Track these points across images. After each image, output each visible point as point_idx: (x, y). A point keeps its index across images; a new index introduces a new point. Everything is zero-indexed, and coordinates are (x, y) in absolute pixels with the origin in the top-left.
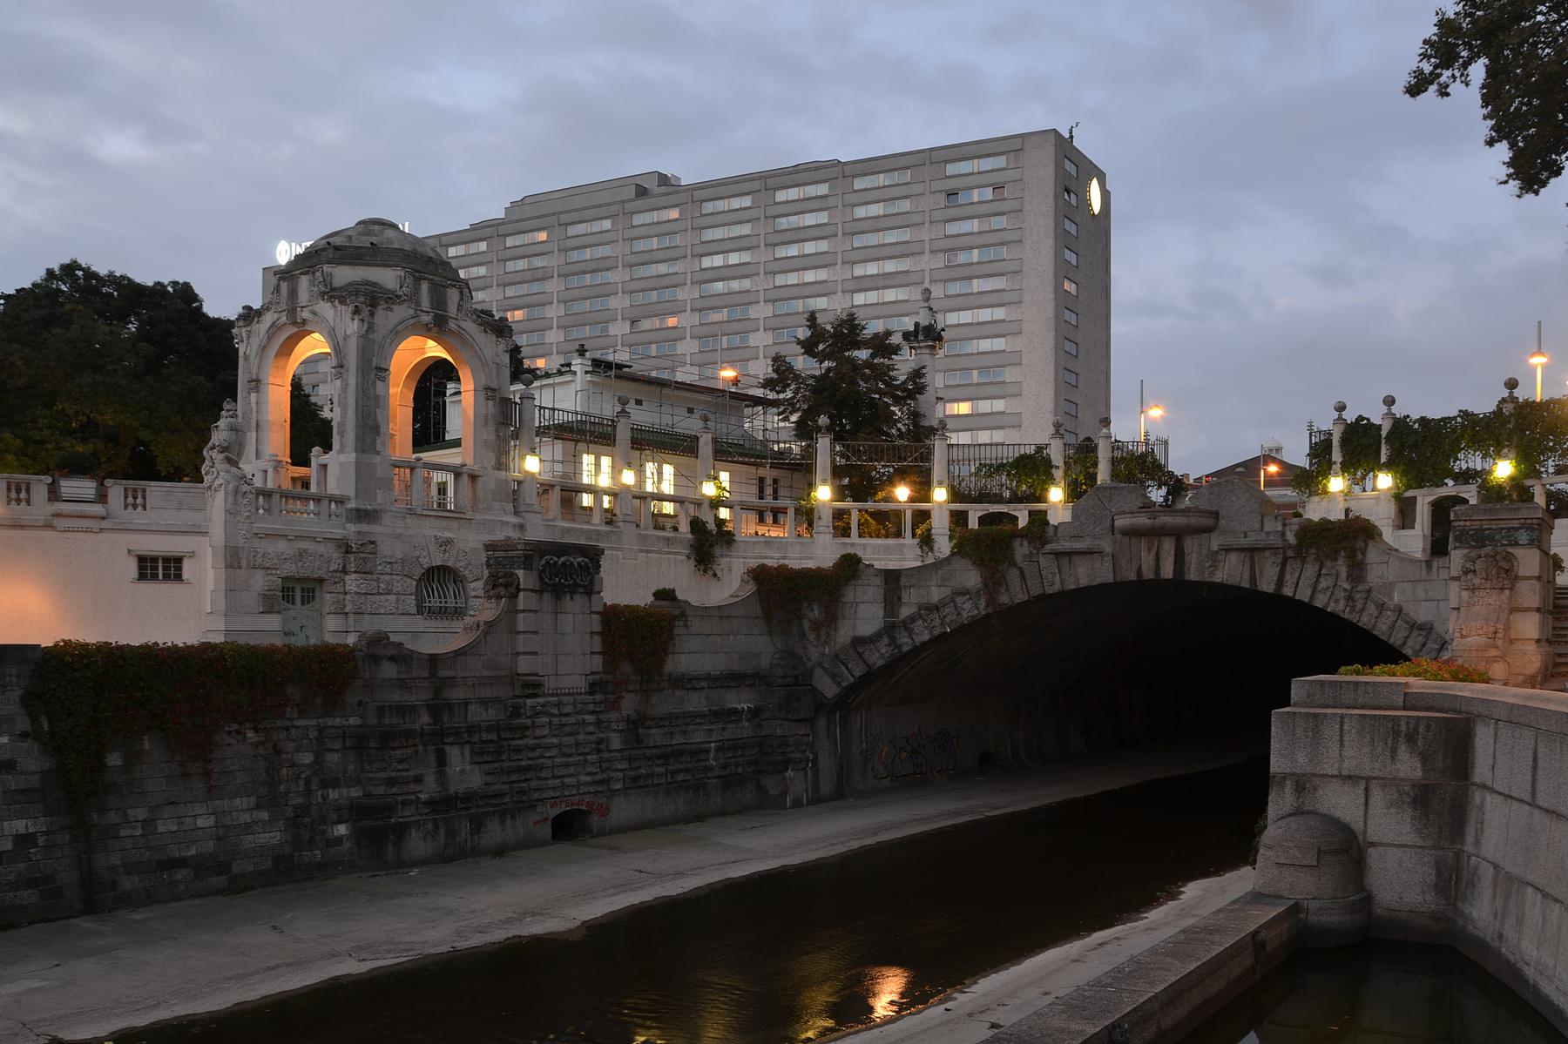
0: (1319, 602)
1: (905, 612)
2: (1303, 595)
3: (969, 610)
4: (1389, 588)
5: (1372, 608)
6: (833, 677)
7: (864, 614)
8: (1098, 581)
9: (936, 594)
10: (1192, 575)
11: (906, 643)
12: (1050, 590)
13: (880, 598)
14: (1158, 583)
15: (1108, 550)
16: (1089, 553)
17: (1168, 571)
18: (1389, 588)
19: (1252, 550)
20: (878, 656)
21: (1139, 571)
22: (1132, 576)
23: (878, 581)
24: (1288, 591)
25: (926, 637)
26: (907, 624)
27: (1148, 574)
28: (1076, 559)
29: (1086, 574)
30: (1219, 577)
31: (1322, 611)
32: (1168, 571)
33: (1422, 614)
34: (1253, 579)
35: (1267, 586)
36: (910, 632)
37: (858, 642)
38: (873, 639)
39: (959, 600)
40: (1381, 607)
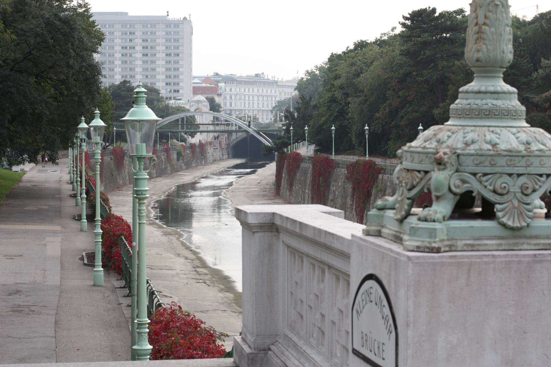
20: (235, 142)
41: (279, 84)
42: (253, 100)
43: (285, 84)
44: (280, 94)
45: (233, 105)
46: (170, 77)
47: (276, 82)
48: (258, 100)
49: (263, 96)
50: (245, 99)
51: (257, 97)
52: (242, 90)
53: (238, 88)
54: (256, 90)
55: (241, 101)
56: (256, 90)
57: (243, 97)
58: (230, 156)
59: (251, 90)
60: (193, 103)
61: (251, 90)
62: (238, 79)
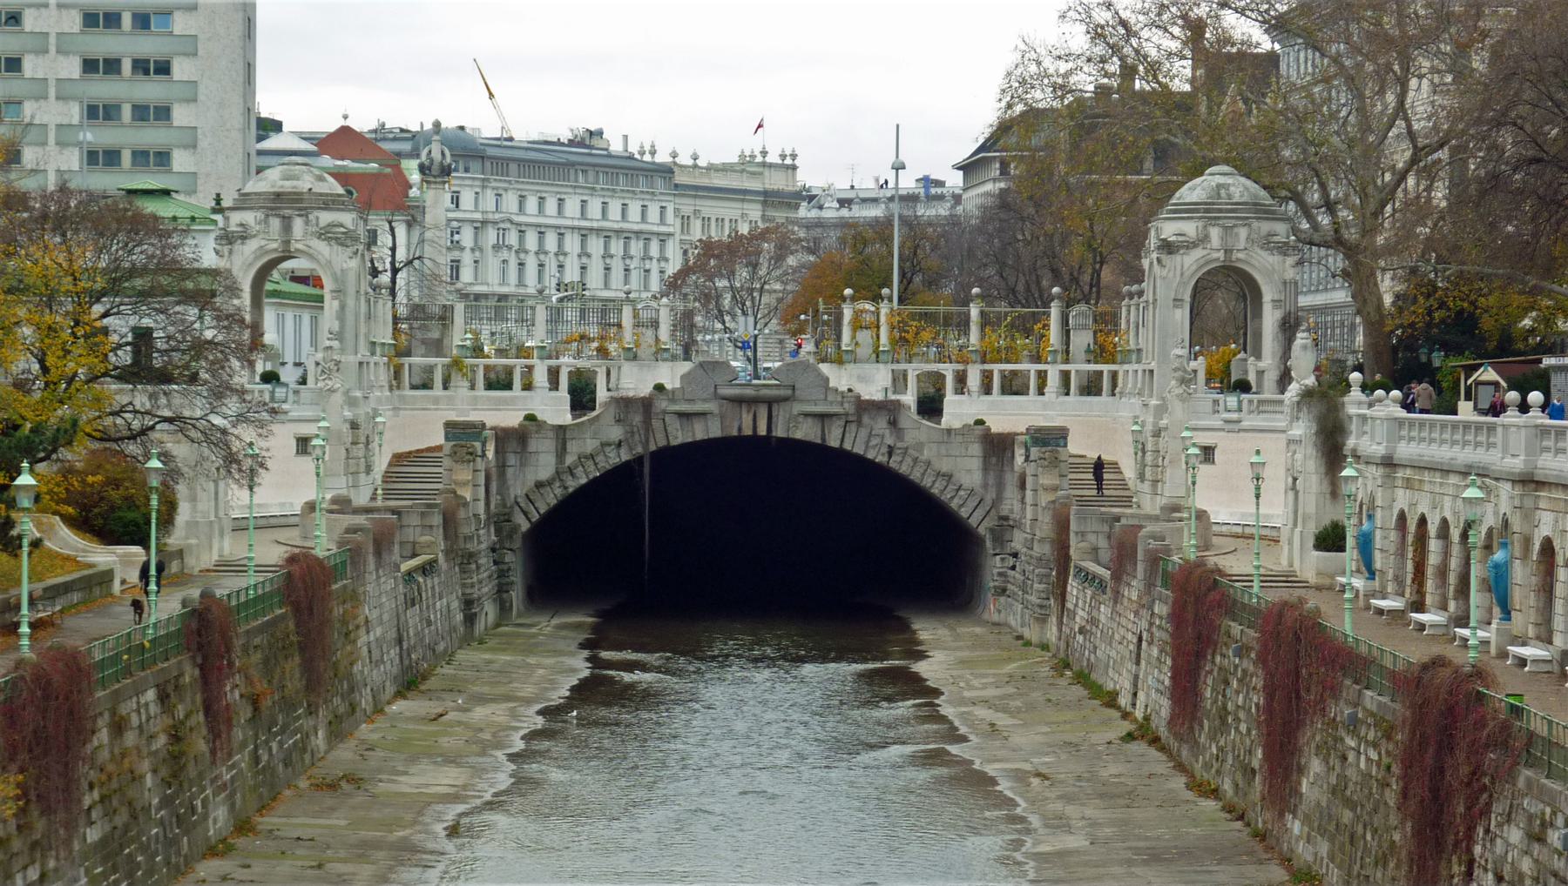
0: (870, 456)
1: (570, 460)
2: (859, 449)
3: (614, 458)
4: (920, 446)
5: (909, 460)
6: (525, 514)
7: (543, 464)
8: (712, 436)
9: (590, 445)
10: (779, 432)
11: (573, 485)
12: (674, 443)
13: (553, 449)
14: (755, 437)
15: (716, 411)
16: (703, 414)
17: (762, 430)
18: (920, 446)
19: (823, 417)
20: (551, 498)
21: (740, 429)
22: (735, 433)
23: (551, 434)
24: (847, 446)
25: (584, 481)
26: (571, 471)
27: (748, 432)
28: (695, 420)
29: (699, 432)
30: (799, 435)
31: (872, 463)
32: (762, 431)
33: (945, 466)
34: (823, 439)
35: (834, 442)
36: (572, 475)
37: (539, 485)
38: (549, 483)
39: (608, 449)
40: (915, 460)
41: (680, 178)
42: (561, 252)
43: (704, 182)
44: (685, 221)
45: (466, 275)
46: (112, 66)
47: (666, 171)
48: (584, 253)
49: (607, 235)
50: (522, 250)
51: (577, 239)
52: (510, 202)
53: (490, 196)
54: (572, 206)
55: (505, 254)
56: (572, 206)
57: (512, 238)
58: (516, 596)
59: (551, 206)
60: (249, 217)
61: (551, 206)
62: (491, 152)
